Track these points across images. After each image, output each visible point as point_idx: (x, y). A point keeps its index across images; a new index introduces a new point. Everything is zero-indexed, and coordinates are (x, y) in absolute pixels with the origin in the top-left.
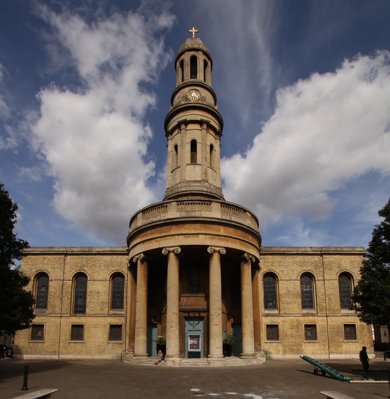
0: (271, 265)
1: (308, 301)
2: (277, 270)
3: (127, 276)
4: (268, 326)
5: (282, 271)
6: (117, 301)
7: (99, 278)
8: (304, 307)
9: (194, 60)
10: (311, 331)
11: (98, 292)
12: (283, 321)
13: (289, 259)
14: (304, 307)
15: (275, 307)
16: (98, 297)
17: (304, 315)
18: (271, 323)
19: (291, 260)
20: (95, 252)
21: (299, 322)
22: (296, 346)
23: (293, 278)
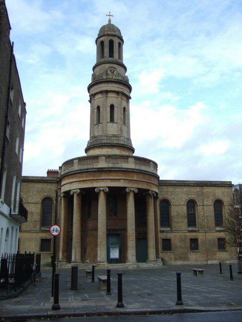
1: (192, 220)
2: (170, 197)
3: (57, 200)
4: (163, 240)
5: (174, 199)
6: (46, 220)
7: (33, 201)
8: (189, 225)
9: (111, 43)
10: (194, 244)
11: (32, 213)
12: (175, 236)
13: (178, 190)
14: (189, 225)
16: (32, 217)
17: (190, 231)
19: (180, 190)
21: (186, 236)
22: (183, 255)
23: (181, 204)
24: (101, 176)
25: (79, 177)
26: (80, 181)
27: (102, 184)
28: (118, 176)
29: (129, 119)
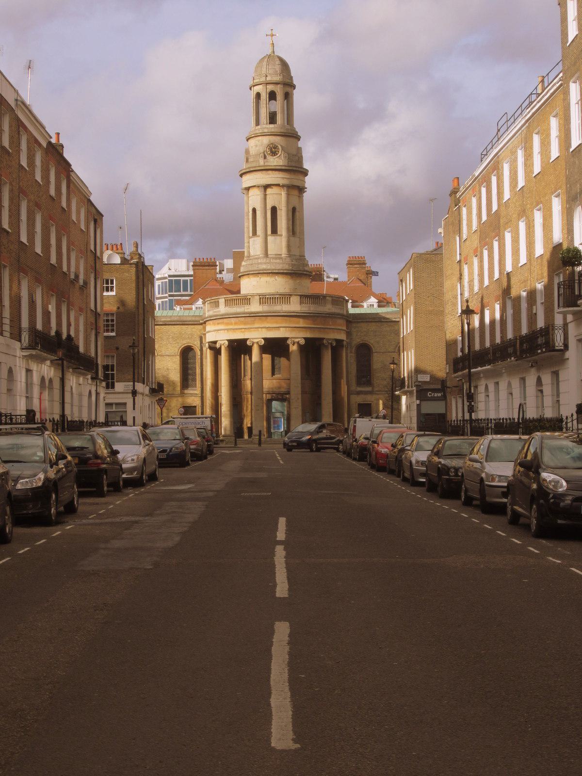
0: (365, 335)
2: (371, 341)
3: (201, 350)
4: (360, 405)
11: (168, 369)
15: (369, 383)
18: (363, 402)
20: (162, 323)
24: (254, 323)
25: (227, 324)
26: (227, 330)
27: (256, 335)
28: (277, 323)
29: (302, 225)
